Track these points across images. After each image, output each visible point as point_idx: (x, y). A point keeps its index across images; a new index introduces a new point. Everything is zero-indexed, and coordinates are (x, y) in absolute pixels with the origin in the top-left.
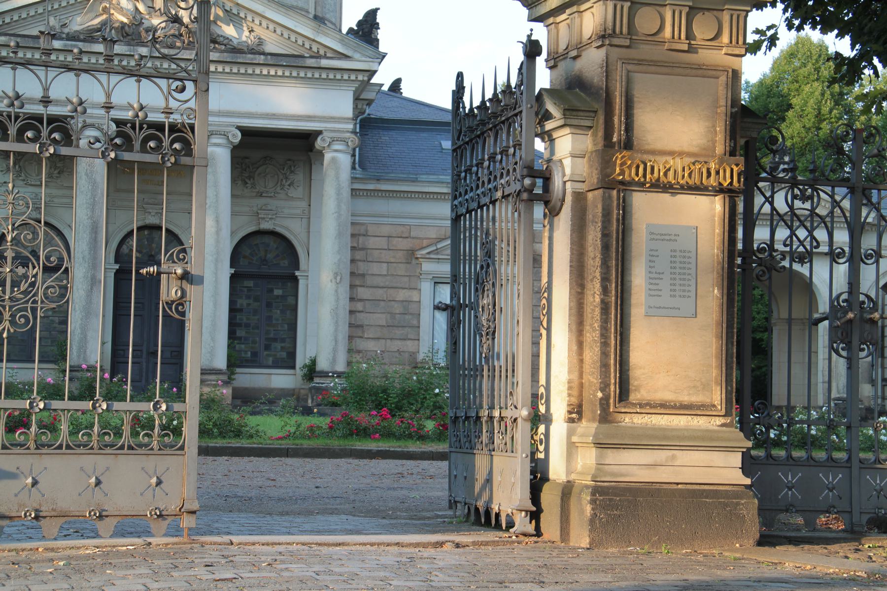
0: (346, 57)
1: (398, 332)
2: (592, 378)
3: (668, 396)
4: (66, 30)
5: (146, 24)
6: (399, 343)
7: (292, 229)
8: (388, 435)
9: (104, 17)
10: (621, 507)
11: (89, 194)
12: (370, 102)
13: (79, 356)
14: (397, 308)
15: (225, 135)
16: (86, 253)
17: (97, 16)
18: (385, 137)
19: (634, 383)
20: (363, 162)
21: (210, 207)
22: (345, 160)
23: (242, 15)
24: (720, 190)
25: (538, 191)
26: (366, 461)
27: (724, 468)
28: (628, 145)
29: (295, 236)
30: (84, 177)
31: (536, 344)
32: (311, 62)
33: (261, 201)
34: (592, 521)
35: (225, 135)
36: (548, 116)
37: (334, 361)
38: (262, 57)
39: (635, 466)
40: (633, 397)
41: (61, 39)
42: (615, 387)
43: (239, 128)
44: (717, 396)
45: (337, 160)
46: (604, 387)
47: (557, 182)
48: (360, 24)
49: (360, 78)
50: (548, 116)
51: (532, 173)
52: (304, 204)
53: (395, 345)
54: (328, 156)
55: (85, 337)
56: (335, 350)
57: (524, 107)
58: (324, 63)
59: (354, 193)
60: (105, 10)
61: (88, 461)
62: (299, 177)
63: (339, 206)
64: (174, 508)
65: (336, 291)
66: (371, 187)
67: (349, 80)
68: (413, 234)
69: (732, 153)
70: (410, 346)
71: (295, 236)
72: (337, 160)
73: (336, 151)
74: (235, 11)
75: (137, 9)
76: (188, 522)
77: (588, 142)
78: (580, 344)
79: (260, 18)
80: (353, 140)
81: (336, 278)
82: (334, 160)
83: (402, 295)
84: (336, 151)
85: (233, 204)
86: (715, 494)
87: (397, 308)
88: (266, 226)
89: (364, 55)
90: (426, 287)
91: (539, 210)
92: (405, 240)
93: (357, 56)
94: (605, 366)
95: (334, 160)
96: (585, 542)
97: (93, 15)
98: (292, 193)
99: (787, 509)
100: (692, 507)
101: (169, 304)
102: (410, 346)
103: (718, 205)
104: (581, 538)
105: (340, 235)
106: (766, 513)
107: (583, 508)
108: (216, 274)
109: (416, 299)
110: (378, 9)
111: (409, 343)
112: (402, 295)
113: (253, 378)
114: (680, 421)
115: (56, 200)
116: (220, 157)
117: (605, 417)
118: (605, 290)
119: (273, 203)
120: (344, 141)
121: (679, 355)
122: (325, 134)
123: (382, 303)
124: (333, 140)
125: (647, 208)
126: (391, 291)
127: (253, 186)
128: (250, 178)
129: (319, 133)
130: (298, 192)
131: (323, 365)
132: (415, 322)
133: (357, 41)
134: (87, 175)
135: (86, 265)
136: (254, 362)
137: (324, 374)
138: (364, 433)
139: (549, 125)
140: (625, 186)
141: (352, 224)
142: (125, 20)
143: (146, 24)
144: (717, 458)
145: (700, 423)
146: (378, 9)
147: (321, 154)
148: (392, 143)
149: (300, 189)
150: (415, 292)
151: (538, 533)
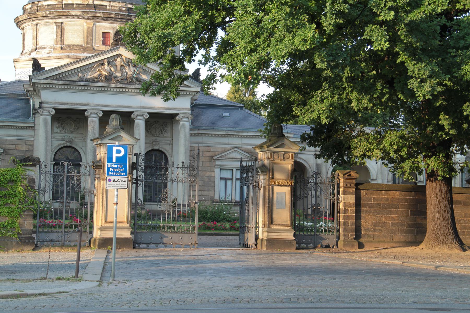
0: (188, 86)
1: (206, 188)
2: (266, 220)
3: (280, 223)
4: (85, 78)
5: (114, 75)
6: (207, 192)
7: (166, 149)
8: (216, 229)
9: (99, 73)
10: (272, 243)
12: (195, 100)
14: (206, 179)
15: (143, 116)
17: (96, 72)
18: (201, 111)
19: (274, 221)
20: (196, 126)
22: (187, 124)
23: (149, 71)
24: (289, 186)
25: (257, 185)
26: (211, 236)
27: (290, 236)
28: (273, 178)
29: (167, 152)
31: (257, 215)
33: (154, 138)
34: (266, 245)
35: (143, 116)
36: (258, 172)
37: (183, 200)
39: (274, 236)
40: (274, 223)
41: (84, 82)
42: (270, 221)
43: (148, 113)
44: (289, 223)
45: (184, 125)
46: (269, 221)
47: (260, 184)
48: (193, 74)
49: (193, 94)
50: (258, 172)
51: (256, 182)
52: (170, 139)
53: (206, 193)
54: (181, 123)
56: (184, 196)
57: (254, 170)
59: (191, 134)
60: (99, 70)
61: (190, 235)
62: (168, 128)
63: (185, 142)
64: (194, 243)
66: (196, 132)
67: (189, 95)
68: (212, 150)
69: (292, 179)
70: (211, 194)
71: (167, 152)
72: (184, 125)
73: (184, 121)
74: (147, 70)
75: (111, 69)
76: (196, 245)
77: (267, 177)
78: (264, 214)
80: (191, 117)
82: (183, 125)
83: (208, 174)
84: (184, 121)
85: (145, 139)
86: (290, 241)
87: (206, 179)
88: (156, 148)
89: (195, 86)
90: (217, 170)
91: (257, 188)
92: (209, 153)
93: (192, 86)
94: (269, 218)
95: (183, 125)
96: (265, 249)
97: (95, 72)
98: (166, 135)
99: (303, 243)
100: (284, 243)
101: (192, 207)
102: (211, 194)
103: (289, 189)
104: (264, 248)
105: (186, 153)
106: (299, 243)
107: (265, 243)
109: (213, 175)
111: (211, 192)
112: (208, 174)
113: (153, 206)
114: (282, 228)
115: (76, 139)
116: (140, 124)
117: (269, 227)
118: (269, 204)
119: (159, 139)
120: (187, 117)
121: (283, 215)
122: (180, 115)
124: (183, 117)
125: (276, 189)
126: (204, 172)
127: (151, 132)
128: (149, 129)
129: (178, 114)
130: (168, 134)
131: (180, 201)
132: (213, 184)
133: (192, 80)
136: (150, 200)
137: (179, 205)
138: (209, 228)
139: (259, 174)
140: (273, 186)
141: (190, 146)
142: (107, 74)
143: (114, 75)
144: (289, 234)
145: (286, 228)
146: (200, 68)
147: (178, 122)
148: (205, 114)
149: (169, 133)
150: (213, 173)
151: (257, 248)
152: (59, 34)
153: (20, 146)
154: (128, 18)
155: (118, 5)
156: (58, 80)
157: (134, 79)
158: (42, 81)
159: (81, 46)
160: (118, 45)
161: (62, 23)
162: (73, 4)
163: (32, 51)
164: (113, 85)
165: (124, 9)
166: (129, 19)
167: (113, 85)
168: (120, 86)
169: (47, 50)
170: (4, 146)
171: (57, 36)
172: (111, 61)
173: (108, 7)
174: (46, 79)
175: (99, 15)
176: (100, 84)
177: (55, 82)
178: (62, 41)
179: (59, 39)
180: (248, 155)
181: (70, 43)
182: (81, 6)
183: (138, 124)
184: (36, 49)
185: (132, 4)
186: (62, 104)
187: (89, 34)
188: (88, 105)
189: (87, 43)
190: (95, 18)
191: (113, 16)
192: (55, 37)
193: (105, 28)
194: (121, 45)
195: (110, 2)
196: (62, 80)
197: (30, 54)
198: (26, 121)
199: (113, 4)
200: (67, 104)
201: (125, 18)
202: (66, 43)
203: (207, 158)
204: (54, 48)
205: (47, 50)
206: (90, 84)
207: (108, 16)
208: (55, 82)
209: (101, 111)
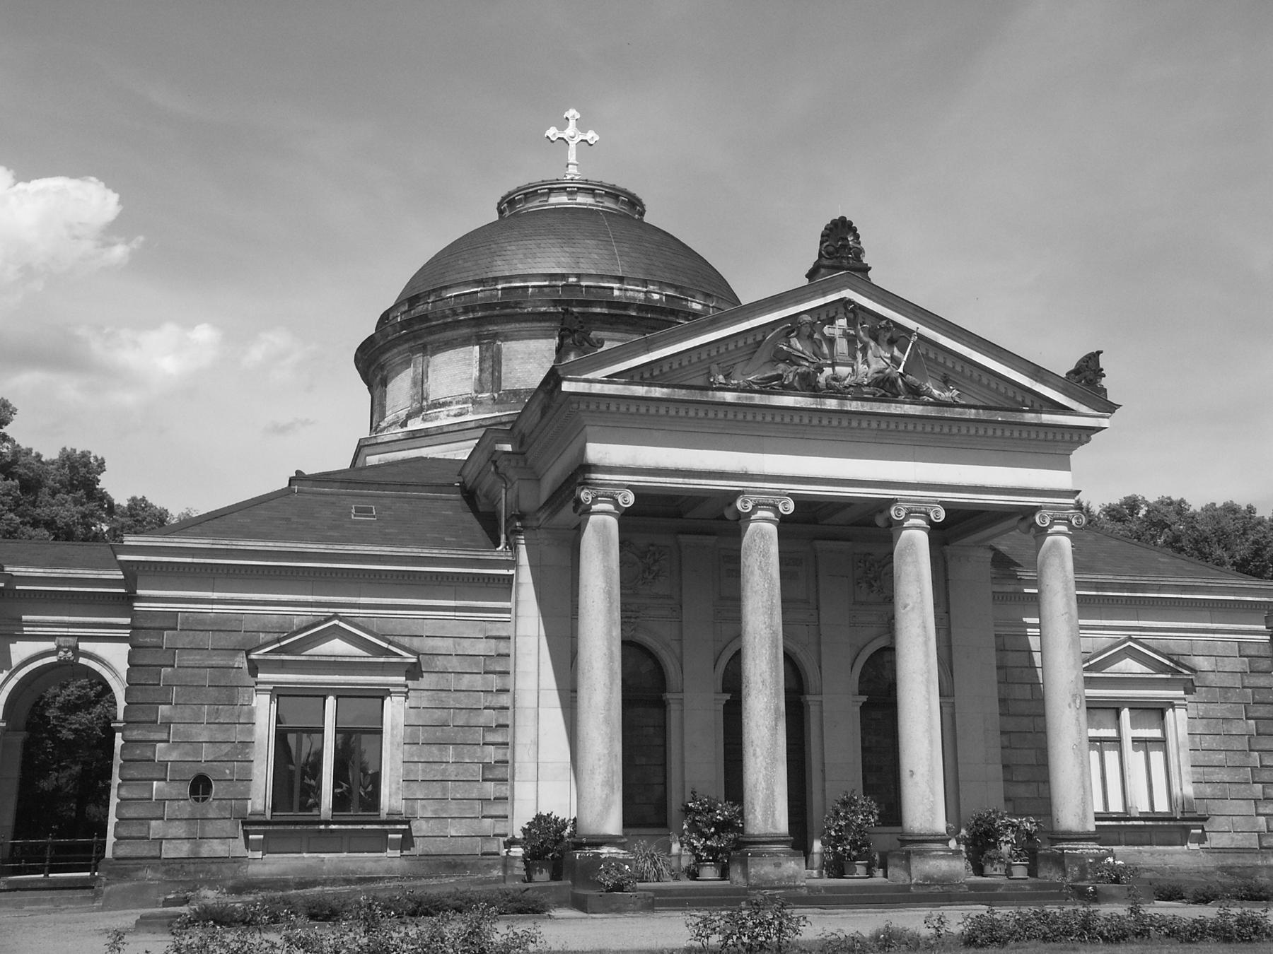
11: (766, 594)
13: (765, 821)
16: (767, 676)
21: (913, 608)
30: (757, 572)
38: (973, 411)
55: (773, 792)
58: (1047, 418)
65: (1077, 720)
79: (962, 363)
81: (1074, 701)
82: (1055, 543)
93: (1083, 409)
95: (1055, 543)
108: (928, 699)
110: (1099, 353)
123: (1029, 736)
134: (761, 568)
135: (768, 692)
146: (1099, 353)
152: (488, 364)
153: (466, 643)
156: (650, 385)
158: (596, 388)
162: (527, 287)
163: (409, 416)
164: (832, 404)
165: (656, 297)
167: (832, 404)
169: (455, 408)
170: (416, 643)
171: (481, 370)
173: (616, 293)
174: (610, 379)
177: (640, 391)
178: (497, 381)
179: (487, 375)
180: (1167, 662)
181: (517, 387)
182: (546, 290)
183: (911, 543)
184: (421, 410)
192: (476, 373)
196: (662, 386)
197: (404, 424)
198: (488, 555)
202: (507, 385)
204: (474, 402)
205: (455, 408)
206: (758, 399)
208: (640, 391)
209: (789, 495)
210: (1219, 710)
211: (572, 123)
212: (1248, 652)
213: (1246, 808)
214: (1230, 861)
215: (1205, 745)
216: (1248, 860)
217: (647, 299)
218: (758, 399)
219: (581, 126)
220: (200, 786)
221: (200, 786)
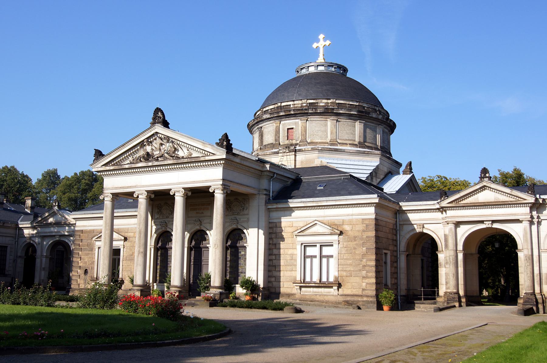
6: (289, 272)
32: (202, 159)
58: (207, 158)
93: (218, 153)
126: (286, 250)
150: (295, 250)
154: (306, 111)
155: (300, 102)
157: (166, 155)
159: (272, 144)
160: (155, 123)
161: (261, 127)
164: (150, 164)
165: (304, 105)
166: (307, 113)
168: (156, 163)
172: (149, 141)
173: (292, 106)
175: (281, 114)
176: (140, 165)
185: (314, 99)
186: (116, 188)
187: (277, 132)
188: (135, 187)
189: (276, 140)
190: (280, 118)
191: (292, 112)
193: (289, 124)
194: (158, 123)
195: (294, 101)
199: (295, 102)
200: (121, 188)
201: (303, 112)
203: (289, 234)
207: (289, 113)
210: (352, 244)
211: (322, 40)
212: (365, 222)
213: (358, 280)
214: (348, 299)
215: (345, 257)
216: (356, 299)
217: (302, 106)
218: (133, 166)
219: (325, 39)
220: (86, 272)
221: (86, 272)
